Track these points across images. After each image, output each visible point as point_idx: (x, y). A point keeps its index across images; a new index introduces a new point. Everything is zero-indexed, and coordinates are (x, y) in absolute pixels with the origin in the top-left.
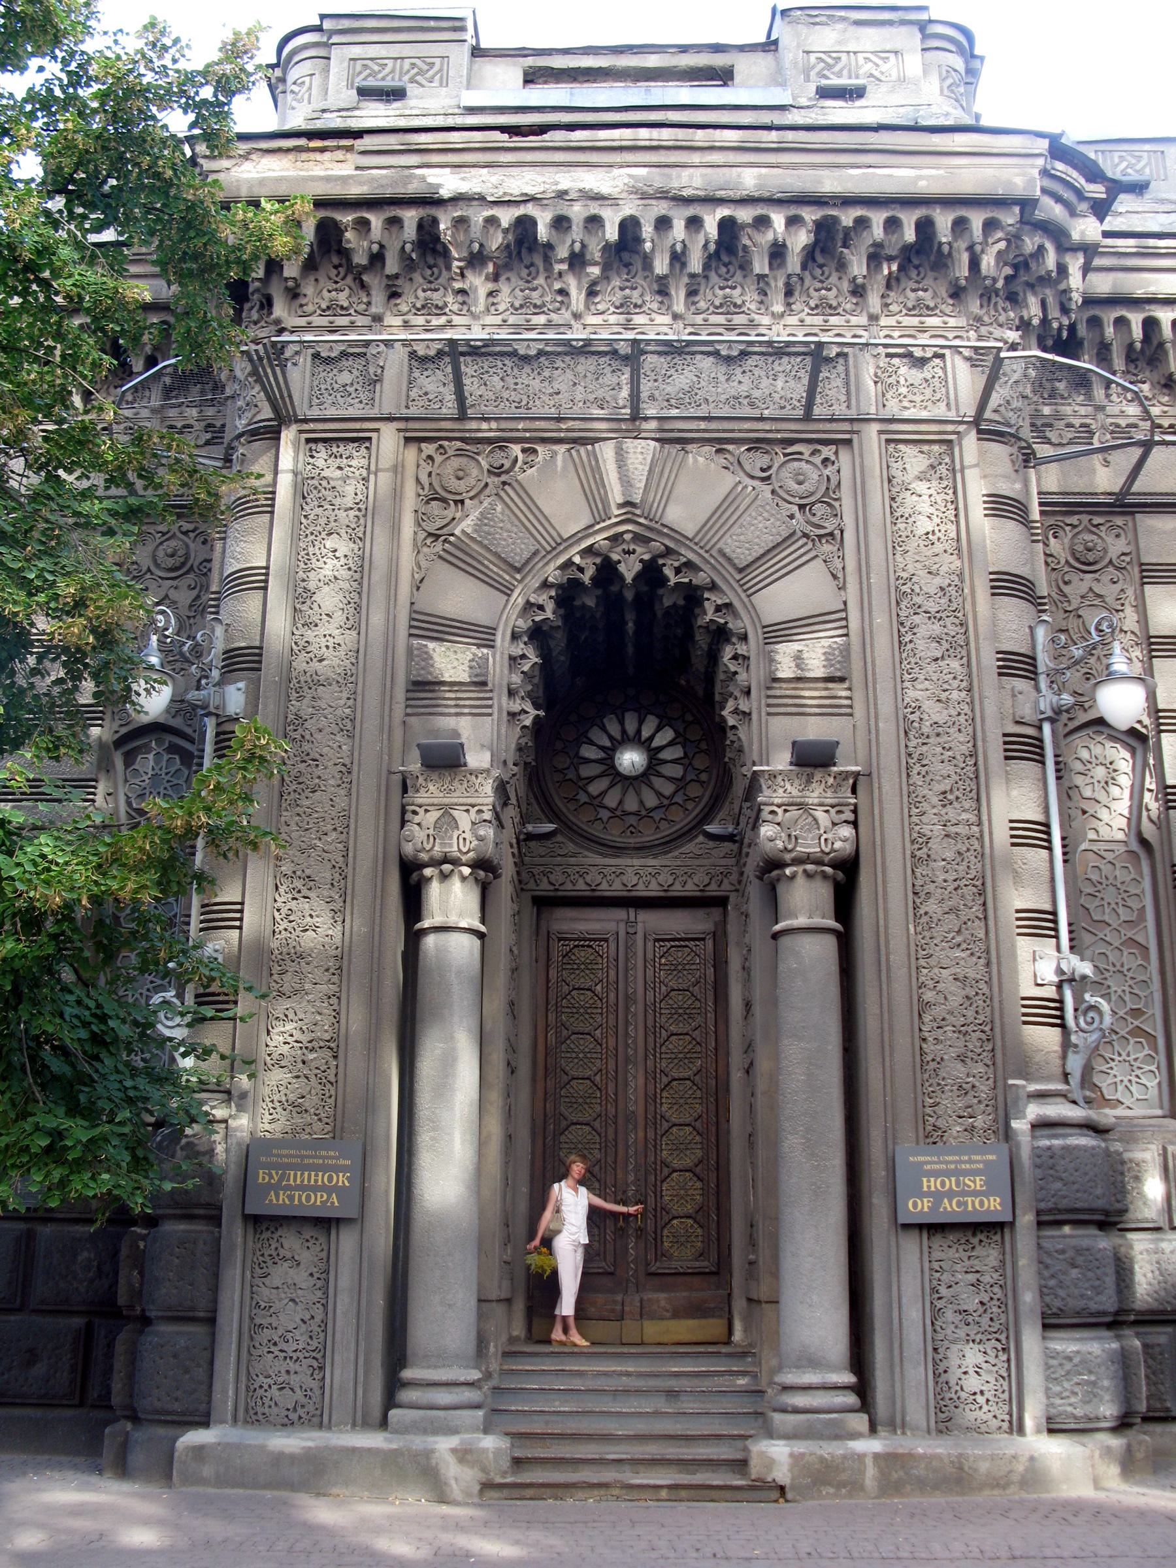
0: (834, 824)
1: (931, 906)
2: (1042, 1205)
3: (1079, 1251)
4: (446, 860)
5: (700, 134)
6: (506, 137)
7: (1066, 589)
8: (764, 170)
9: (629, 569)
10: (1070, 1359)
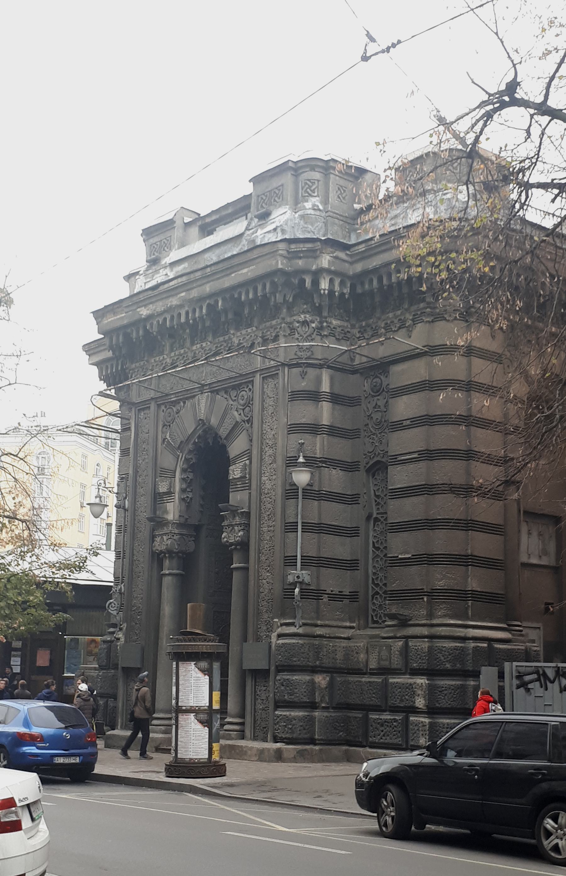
0: (239, 531)
1: (263, 558)
2: (277, 664)
3: (285, 680)
4: (161, 552)
5: (192, 276)
6: (150, 292)
7: (369, 406)
8: (212, 283)
9: (210, 441)
10: (278, 717)
